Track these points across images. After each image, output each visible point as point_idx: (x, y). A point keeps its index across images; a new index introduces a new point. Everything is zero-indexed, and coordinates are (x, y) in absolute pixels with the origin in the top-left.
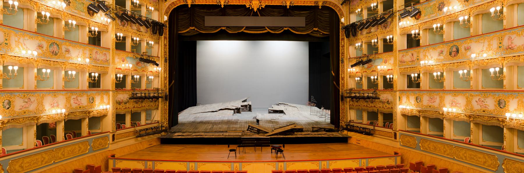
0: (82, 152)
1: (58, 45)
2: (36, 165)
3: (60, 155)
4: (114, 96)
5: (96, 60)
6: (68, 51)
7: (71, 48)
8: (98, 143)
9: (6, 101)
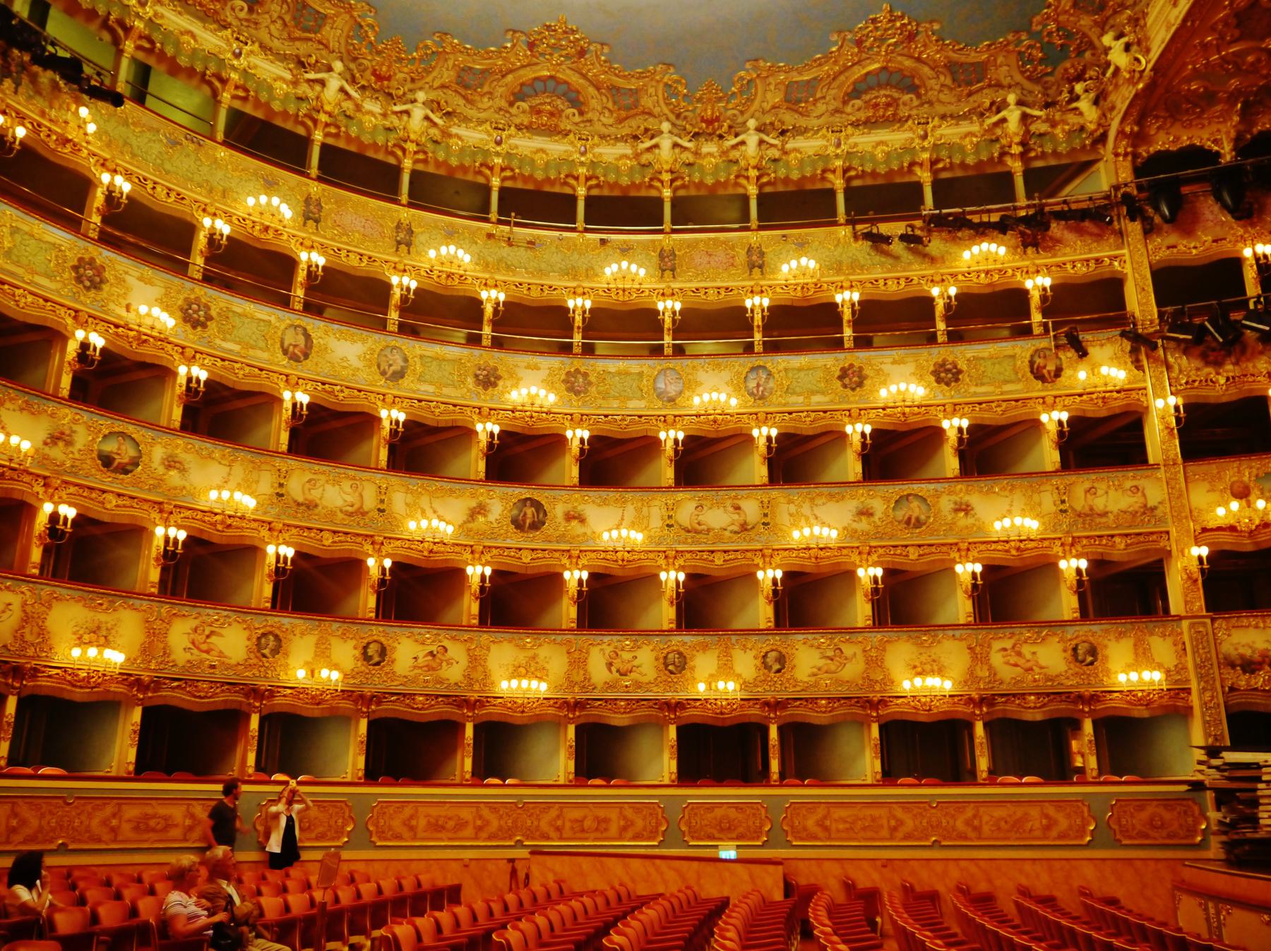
0: (1060, 837)
1: (924, 500)
2: (869, 834)
3: (960, 824)
4: (1199, 639)
5: (1090, 516)
6: (966, 509)
7: (975, 500)
8: (1144, 815)
9: (774, 654)
